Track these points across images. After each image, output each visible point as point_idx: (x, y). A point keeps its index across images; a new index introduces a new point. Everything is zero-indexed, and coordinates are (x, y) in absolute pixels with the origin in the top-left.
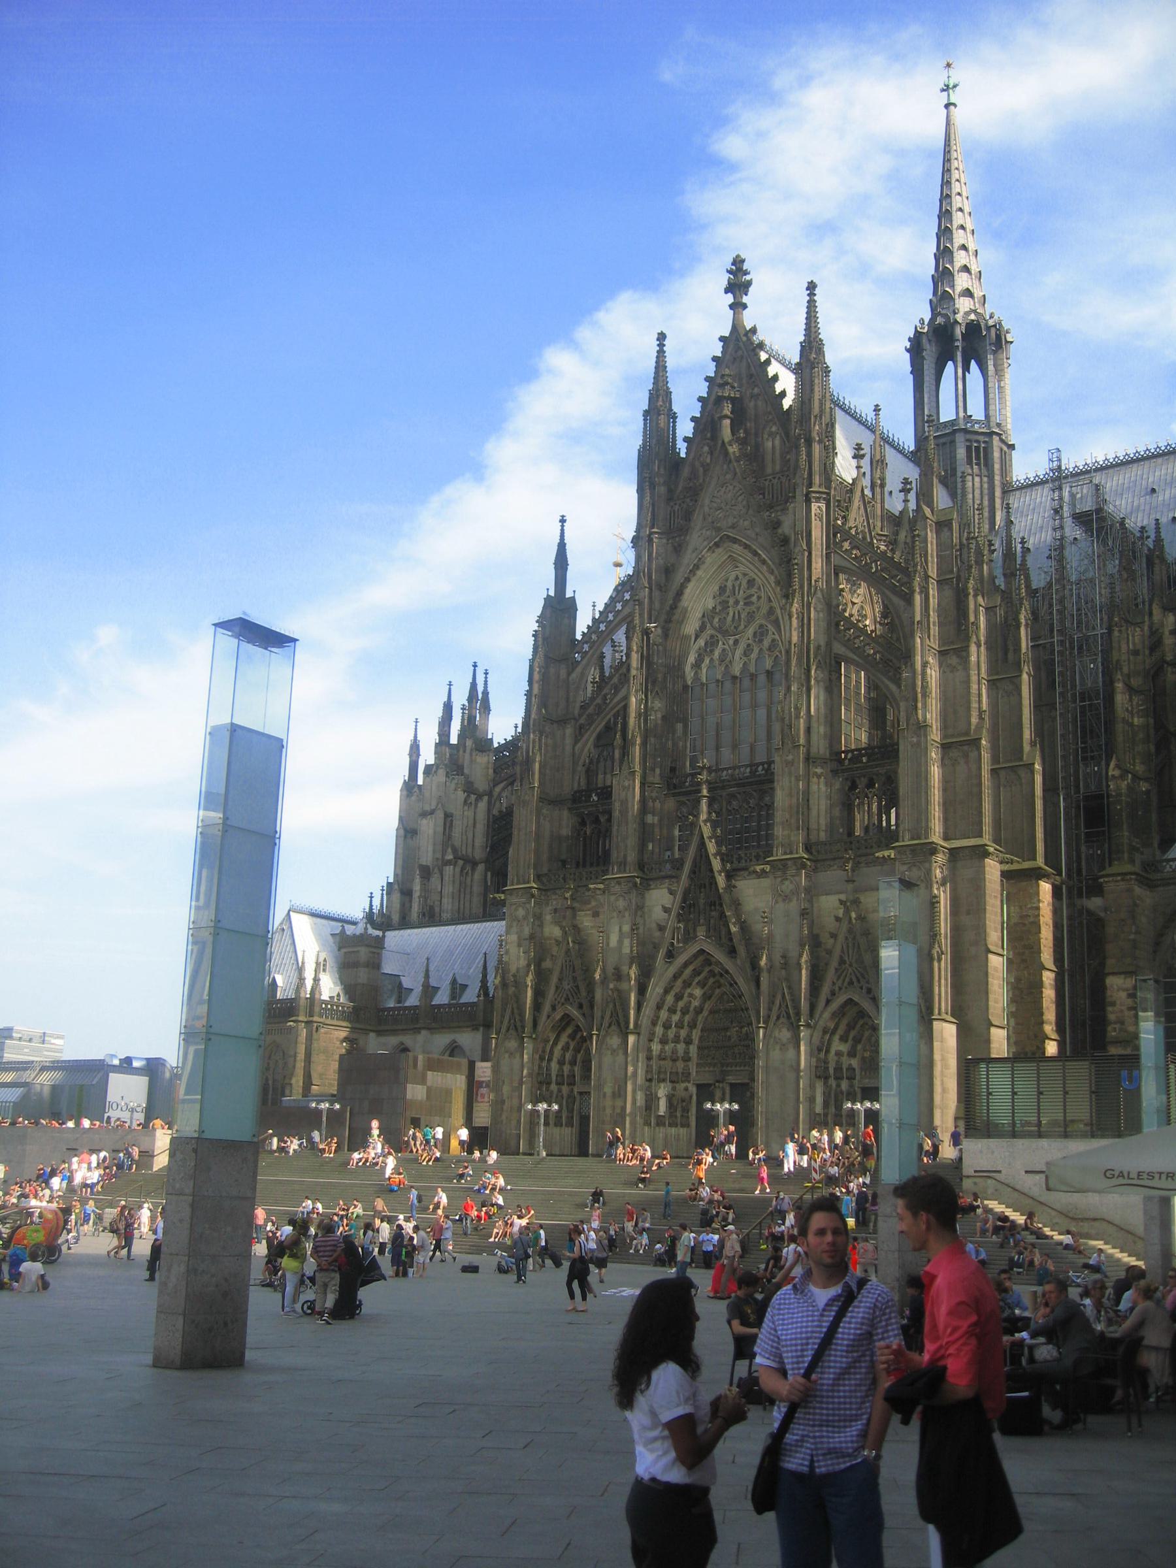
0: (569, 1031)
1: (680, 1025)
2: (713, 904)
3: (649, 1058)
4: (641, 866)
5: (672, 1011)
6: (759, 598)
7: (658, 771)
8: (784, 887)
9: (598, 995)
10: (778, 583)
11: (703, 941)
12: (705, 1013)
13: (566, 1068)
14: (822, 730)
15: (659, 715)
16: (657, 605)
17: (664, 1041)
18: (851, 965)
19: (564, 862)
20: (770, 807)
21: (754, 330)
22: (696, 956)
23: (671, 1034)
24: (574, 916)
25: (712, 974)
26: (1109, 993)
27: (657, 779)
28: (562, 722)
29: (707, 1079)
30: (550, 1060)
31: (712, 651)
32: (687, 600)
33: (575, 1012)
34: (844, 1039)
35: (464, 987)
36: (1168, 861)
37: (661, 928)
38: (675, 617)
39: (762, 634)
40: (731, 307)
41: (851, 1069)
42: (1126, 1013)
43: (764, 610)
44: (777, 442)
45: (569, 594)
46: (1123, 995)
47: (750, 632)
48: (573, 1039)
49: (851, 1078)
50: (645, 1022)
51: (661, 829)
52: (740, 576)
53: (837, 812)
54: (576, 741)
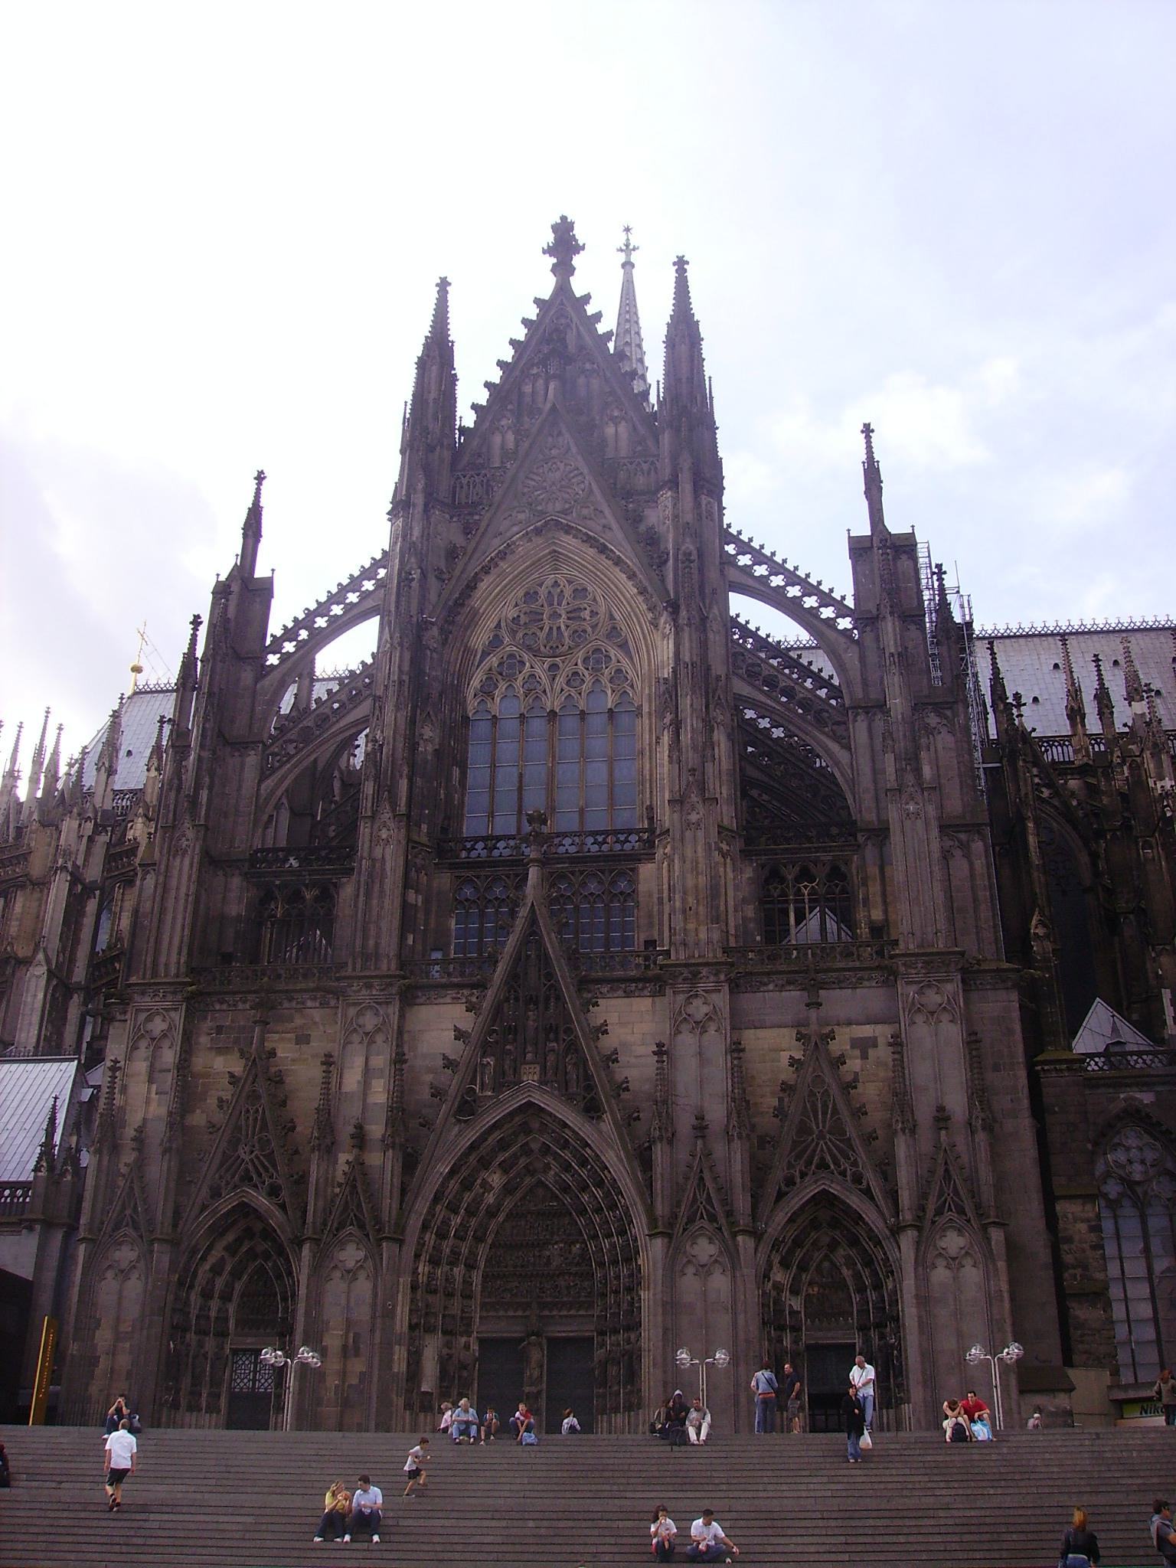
0: (230, 1237)
1: (460, 1237)
2: (551, 1031)
3: (414, 1288)
4: (402, 966)
5: (453, 1209)
6: (593, 614)
7: (424, 827)
8: (691, 1010)
9: (315, 1171)
10: (642, 591)
11: (532, 1087)
12: (501, 1218)
13: (215, 1305)
14: (724, 792)
15: (430, 748)
16: (433, 596)
17: (434, 1262)
18: (821, 1136)
19: (227, 958)
20: (632, 894)
21: (587, 298)
22: (511, 1115)
23: (446, 1247)
24: (262, 1040)
25: (526, 1150)
26: (1061, 1225)
27: (424, 840)
28: (241, 746)
29: (505, 1327)
30: (191, 1287)
31: (510, 678)
32: (476, 600)
33: (261, 1201)
34: (785, 1264)
36: (1092, 1056)
37: (449, 1064)
38: (460, 619)
39: (598, 661)
40: (554, 269)
41: (793, 1313)
42: (1089, 1252)
44: (622, 428)
45: (261, 571)
46: (1083, 1227)
48: (233, 1255)
49: (796, 1329)
50: (415, 1223)
51: (427, 913)
52: (562, 582)
53: (750, 911)
54: (262, 778)
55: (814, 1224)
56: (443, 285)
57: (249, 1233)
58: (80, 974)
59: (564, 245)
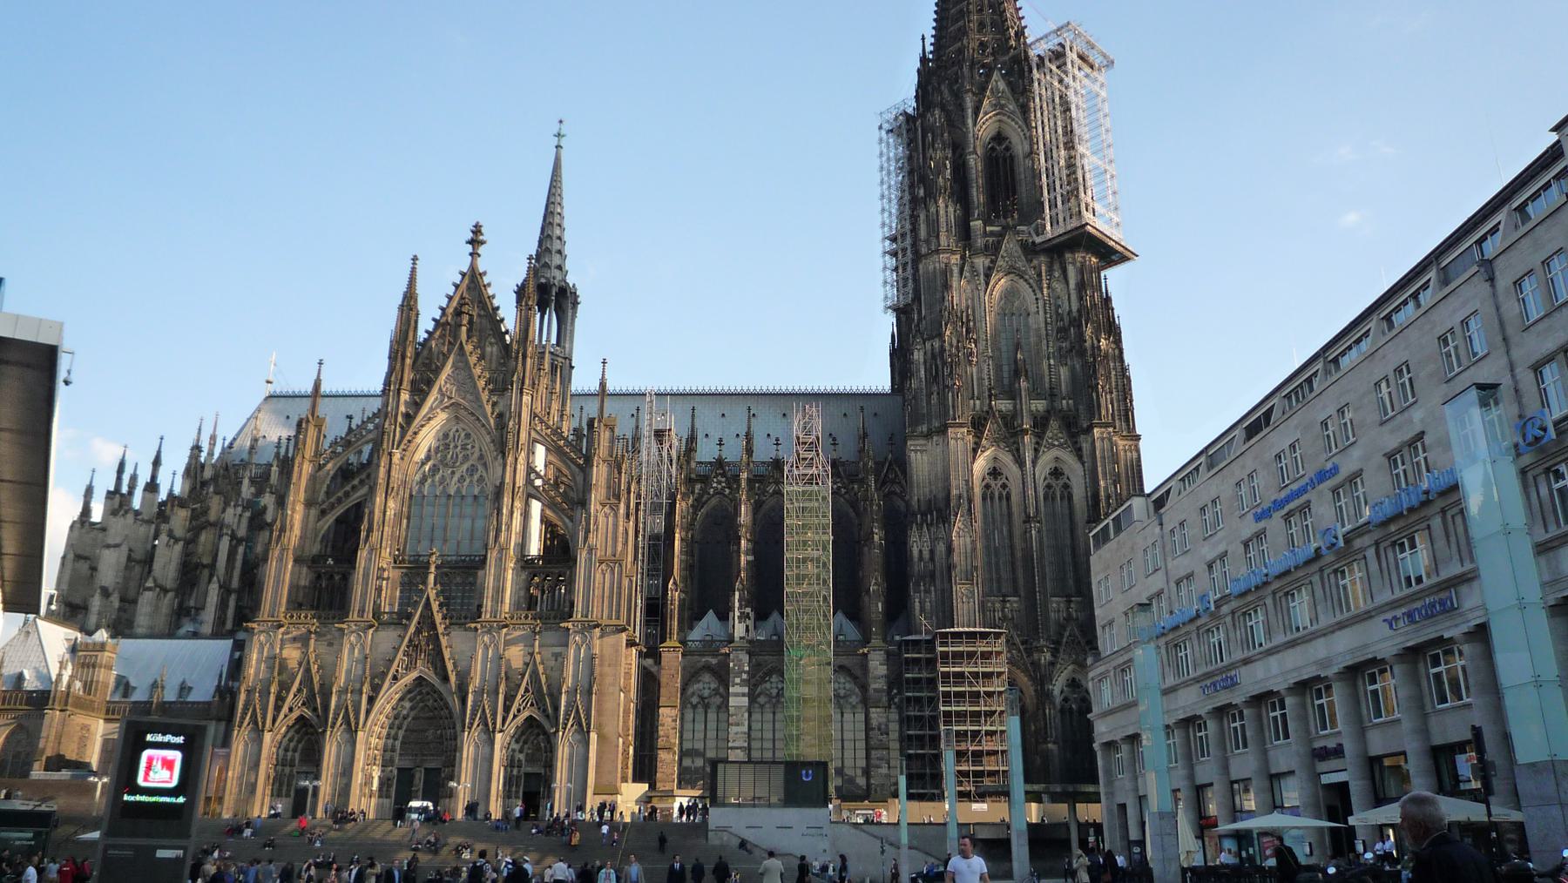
20: (473, 584)
25: (420, 693)
29: (407, 764)
35: (190, 689)
43: (476, 455)
47: (465, 467)
55: (531, 726)
56: (415, 259)
57: (305, 725)
58: (235, 583)
59: (476, 241)
